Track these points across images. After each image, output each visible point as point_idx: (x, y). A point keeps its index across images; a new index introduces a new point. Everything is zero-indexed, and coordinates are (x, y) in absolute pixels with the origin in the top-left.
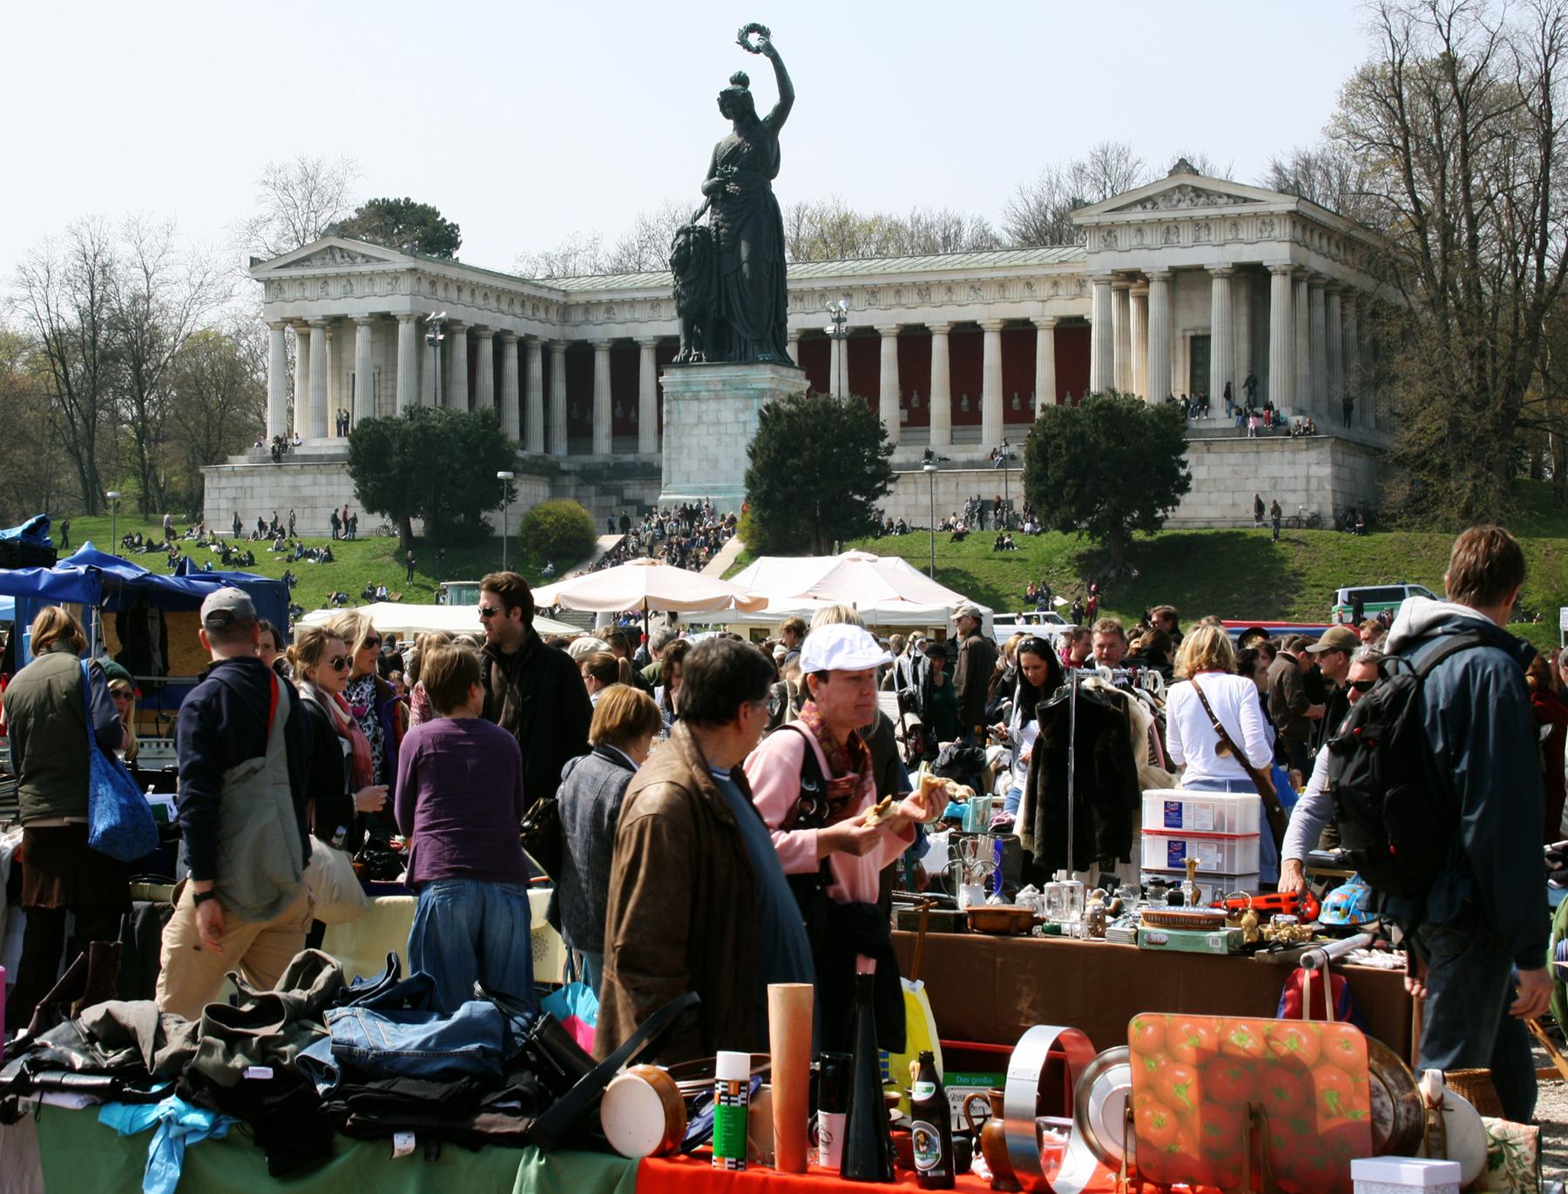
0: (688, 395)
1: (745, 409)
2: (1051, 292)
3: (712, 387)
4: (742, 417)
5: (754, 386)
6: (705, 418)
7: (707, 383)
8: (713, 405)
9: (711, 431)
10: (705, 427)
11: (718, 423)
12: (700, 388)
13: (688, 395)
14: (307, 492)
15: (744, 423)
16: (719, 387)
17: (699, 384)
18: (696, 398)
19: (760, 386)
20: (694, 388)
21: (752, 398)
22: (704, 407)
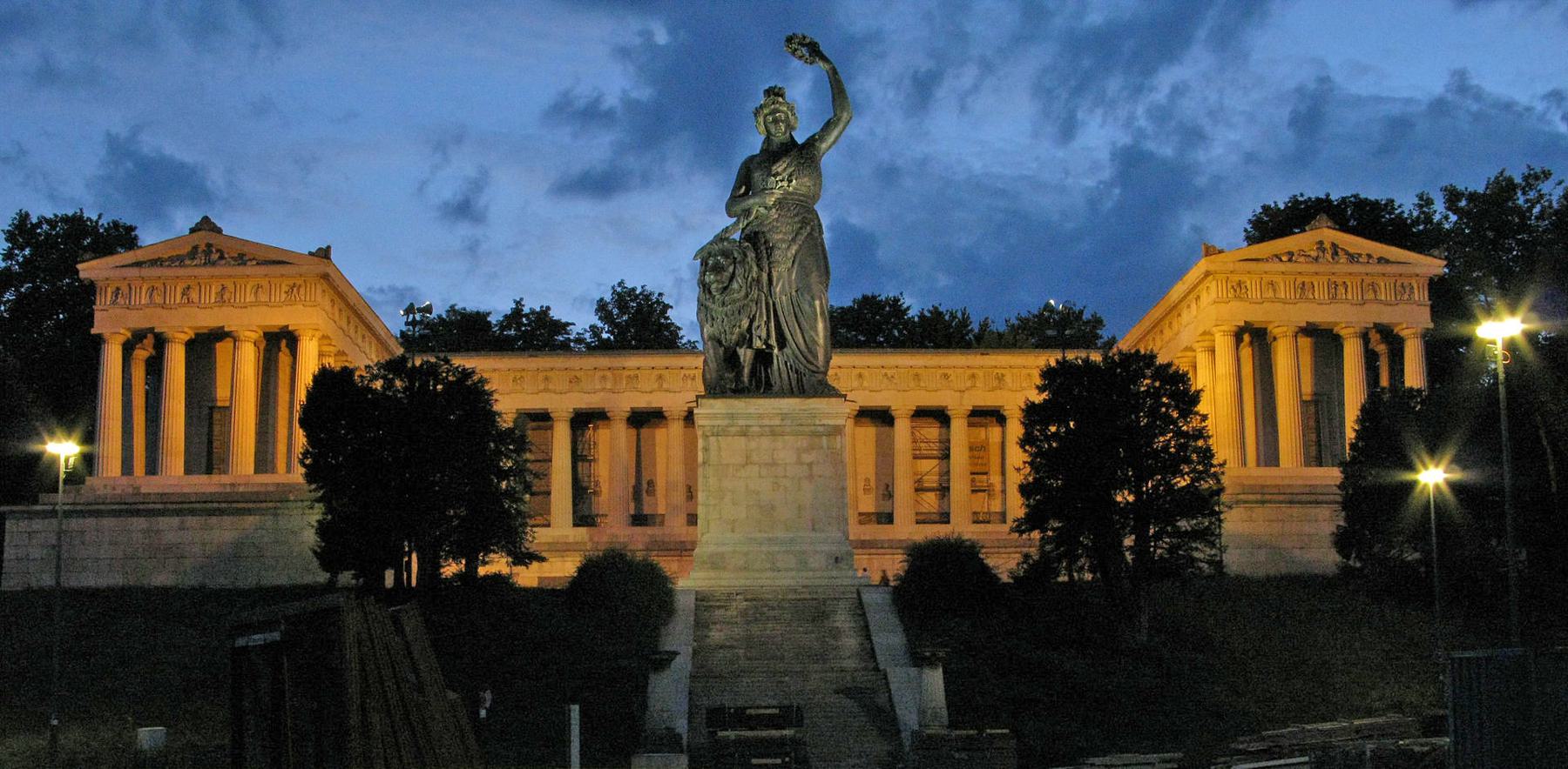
0: (733, 429)
1: (810, 449)
2: (969, 384)
3: (767, 422)
4: (807, 458)
5: (825, 422)
6: (755, 458)
7: (761, 416)
8: (765, 442)
9: (764, 471)
10: (756, 468)
11: (774, 464)
12: (749, 423)
13: (733, 429)
14: (170, 537)
15: (810, 465)
16: (777, 422)
17: (748, 416)
18: (744, 433)
19: (831, 422)
20: (741, 422)
21: (820, 435)
22: (753, 445)
